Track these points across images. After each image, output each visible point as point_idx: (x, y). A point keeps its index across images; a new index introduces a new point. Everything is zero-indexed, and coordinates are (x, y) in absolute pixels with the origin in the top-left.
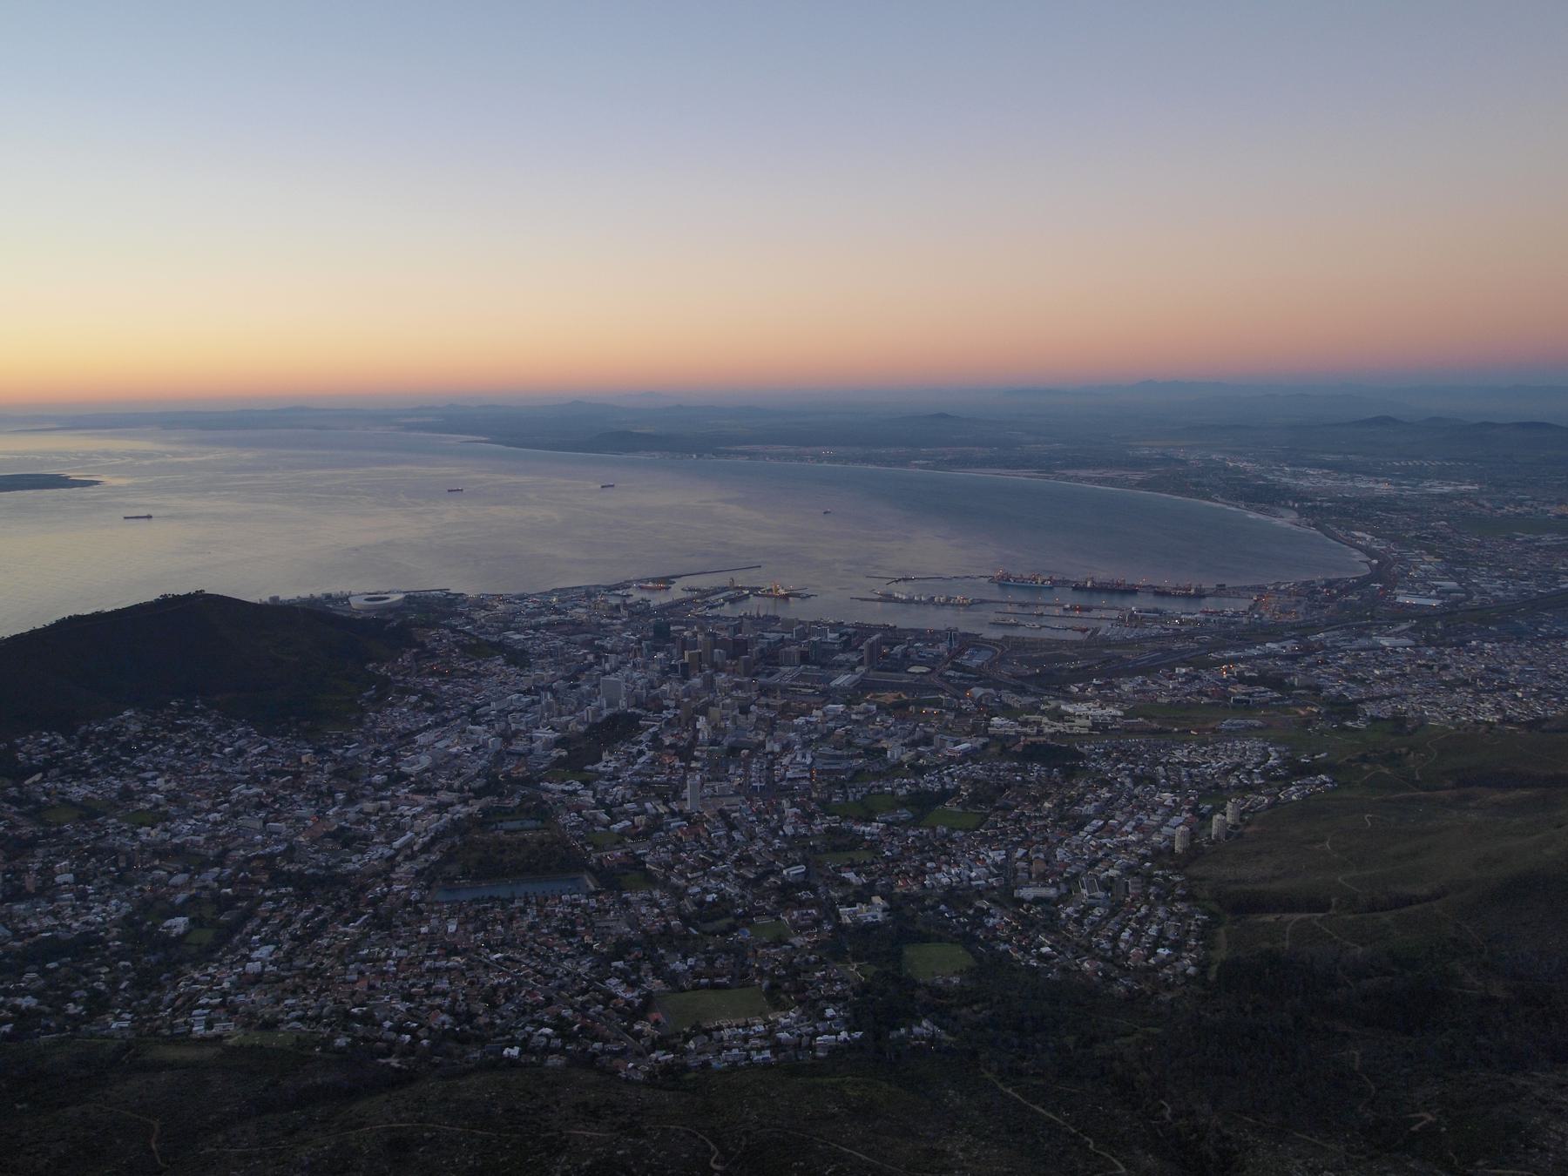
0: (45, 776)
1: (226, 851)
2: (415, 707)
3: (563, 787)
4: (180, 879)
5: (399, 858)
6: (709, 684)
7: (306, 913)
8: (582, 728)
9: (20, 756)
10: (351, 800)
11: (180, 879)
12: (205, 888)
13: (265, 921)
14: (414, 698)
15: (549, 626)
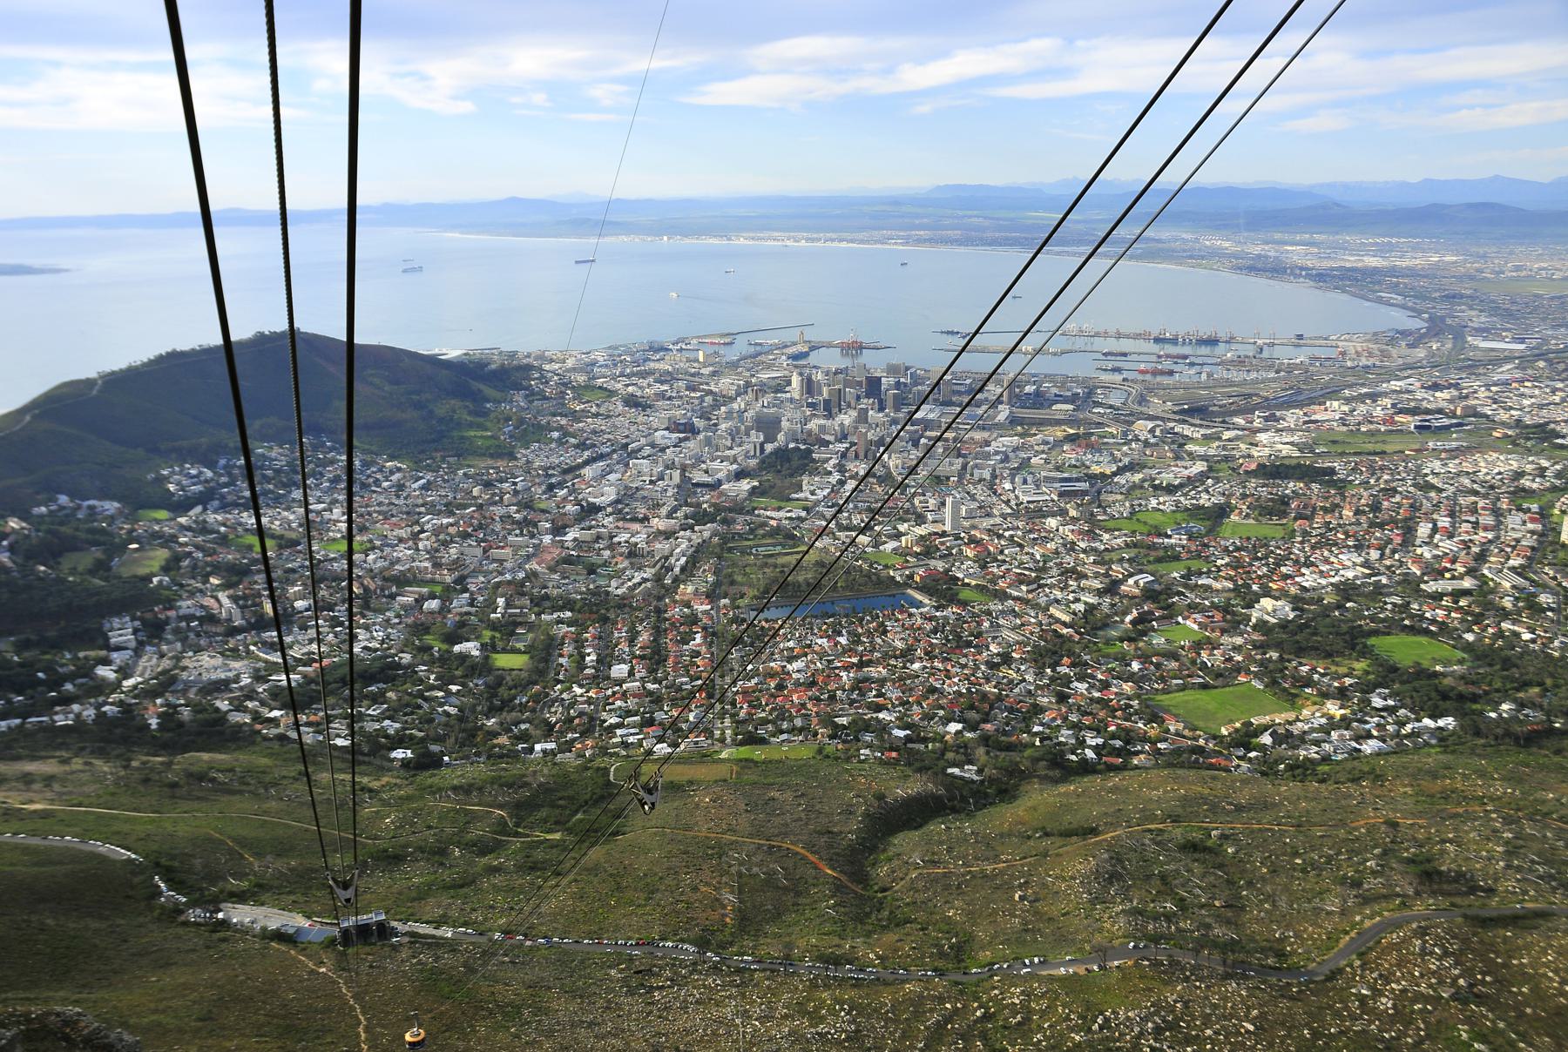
0: (205, 509)
1: (461, 580)
2: (560, 442)
3: (782, 514)
4: (433, 604)
5: (668, 581)
6: (863, 417)
7: (620, 634)
8: (753, 463)
9: (172, 487)
10: (559, 530)
11: (433, 604)
12: (469, 613)
13: (579, 643)
14: (556, 435)
15: (633, 374)
